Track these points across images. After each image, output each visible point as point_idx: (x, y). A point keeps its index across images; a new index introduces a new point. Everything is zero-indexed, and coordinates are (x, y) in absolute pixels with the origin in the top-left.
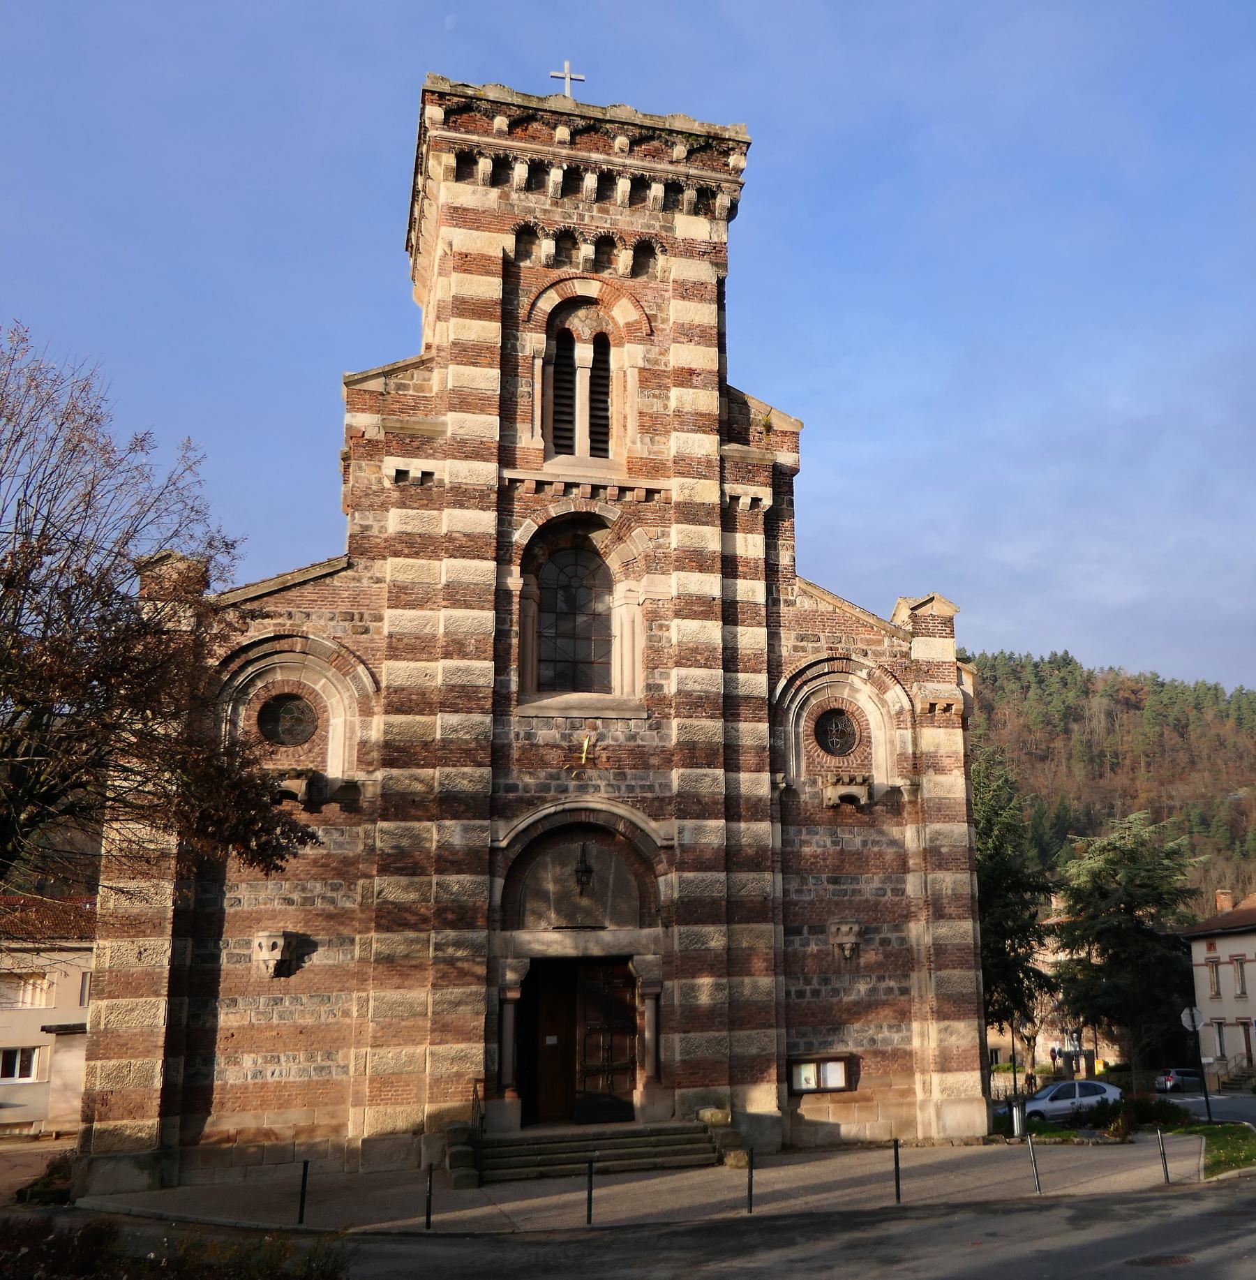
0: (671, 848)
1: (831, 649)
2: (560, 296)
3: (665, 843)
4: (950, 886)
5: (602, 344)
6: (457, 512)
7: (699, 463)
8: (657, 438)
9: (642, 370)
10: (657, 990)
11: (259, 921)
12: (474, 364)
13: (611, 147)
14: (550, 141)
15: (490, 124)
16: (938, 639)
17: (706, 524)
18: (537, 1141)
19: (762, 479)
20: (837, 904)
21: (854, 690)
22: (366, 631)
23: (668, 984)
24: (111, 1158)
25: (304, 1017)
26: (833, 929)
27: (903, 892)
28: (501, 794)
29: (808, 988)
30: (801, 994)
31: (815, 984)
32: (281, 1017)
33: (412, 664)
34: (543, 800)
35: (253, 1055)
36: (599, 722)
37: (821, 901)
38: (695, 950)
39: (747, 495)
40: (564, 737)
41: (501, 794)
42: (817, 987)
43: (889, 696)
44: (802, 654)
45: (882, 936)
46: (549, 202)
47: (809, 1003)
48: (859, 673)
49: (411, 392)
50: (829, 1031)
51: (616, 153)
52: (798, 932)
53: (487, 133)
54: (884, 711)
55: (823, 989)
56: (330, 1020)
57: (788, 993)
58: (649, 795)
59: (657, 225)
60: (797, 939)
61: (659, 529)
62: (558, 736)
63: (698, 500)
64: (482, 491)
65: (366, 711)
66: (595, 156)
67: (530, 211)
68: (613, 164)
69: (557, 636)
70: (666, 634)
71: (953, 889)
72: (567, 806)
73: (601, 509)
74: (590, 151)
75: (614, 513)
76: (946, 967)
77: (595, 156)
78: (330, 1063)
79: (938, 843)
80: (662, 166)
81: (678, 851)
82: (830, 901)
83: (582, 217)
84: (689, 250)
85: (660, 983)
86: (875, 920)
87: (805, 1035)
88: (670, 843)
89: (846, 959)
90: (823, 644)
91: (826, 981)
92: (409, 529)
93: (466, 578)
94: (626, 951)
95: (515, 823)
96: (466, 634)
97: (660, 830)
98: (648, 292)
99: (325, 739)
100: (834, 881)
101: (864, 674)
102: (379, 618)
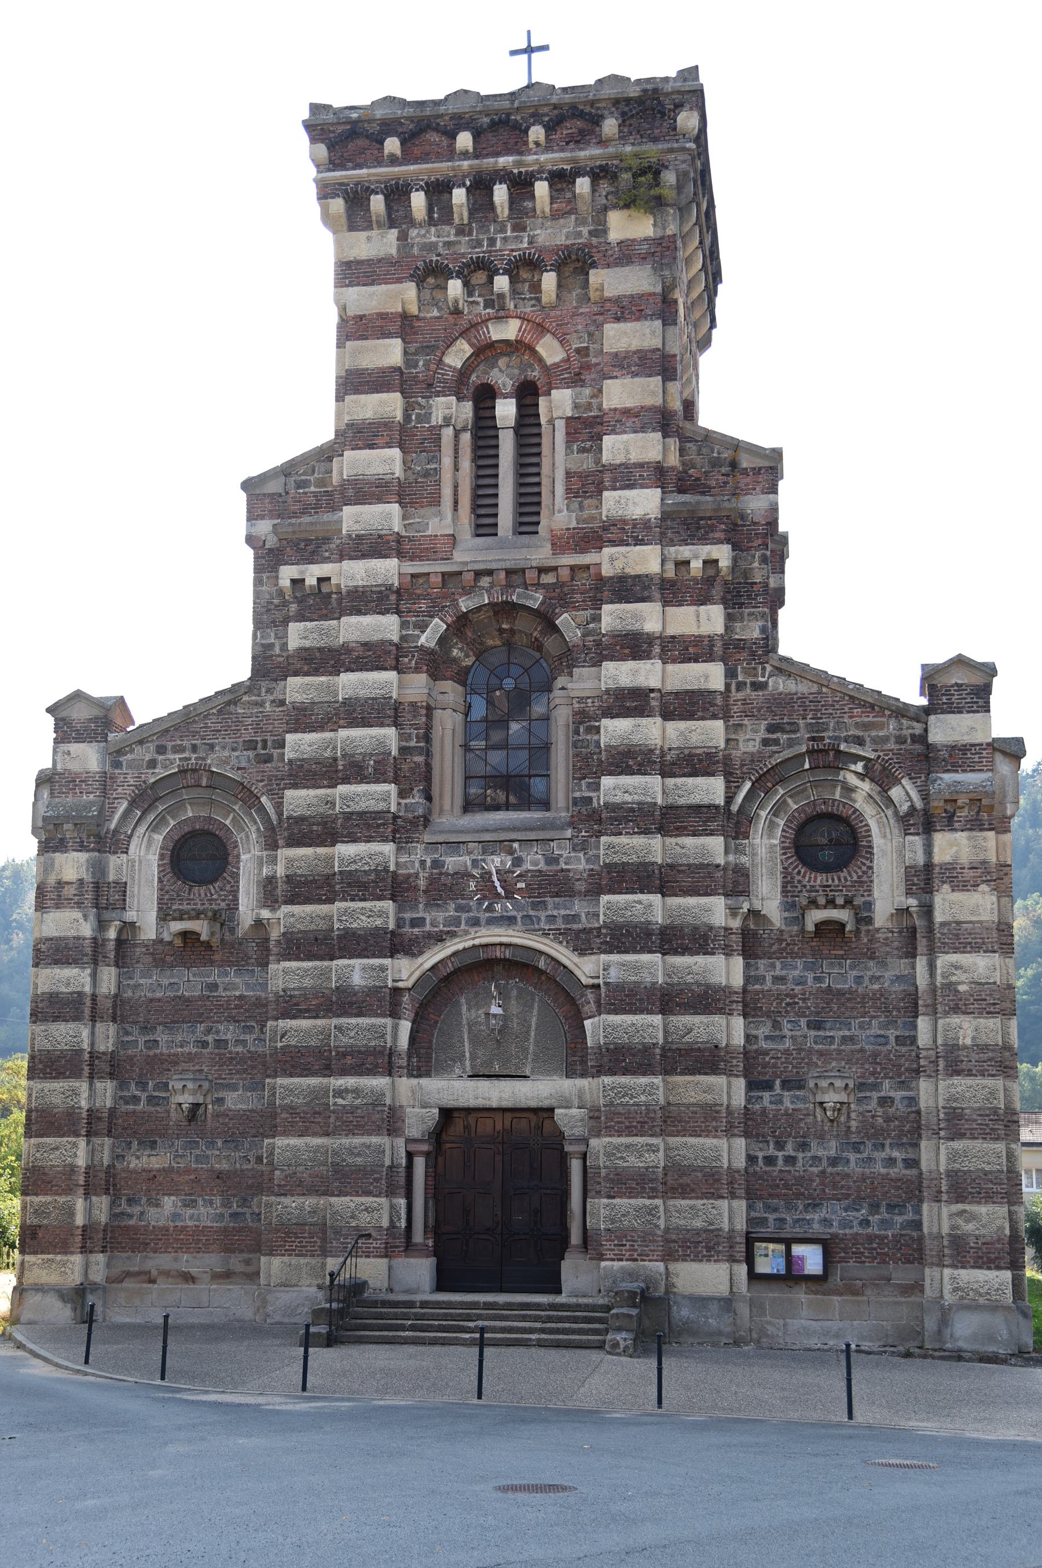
0: (598, 986)
1: (813, 739)
2: (471, 345)
3: (591, 981)
4: (970, 1033)
5: (528, 395)
6: (354, 620)
7: (634, 526)
8: (587, 502)
9: (569, 420)
10: (583, 1148)
11: (176, 1063)
12: (371, 447)
13: (526, 143)
14: (451, 153)
15: (381, 149)
16: (966, 715)
17: (643, 600)
18: (450, 1305)
19: (717, 535)
20: (821, 1054)
21: (849, 790)
22: (268, 759)
23: (594, 1142)
24: (37, 1290)
25: (219, 1162)
26: (811, 1084)
27: (913, 1040)
28: (407, 929)
29: (780, 1154)
30: (770, 1160)
31: (790, 1150)
32: (197, 1161)
33: (312, 792)
34: (453, 934)
35: (173, 1198)
36: (516, 845)
37: (799, 1050)
38: (621, 1104)
39: (696, 557)
40: (475, 863)
41: (407, 929)
42: (793, 1154)
43: (895, 793)
44: (775, 748)
45: (883, 1094)
46: (453, 231)
47: (781, 1171)
48: (853, 767)
49: (312, 489)
50: (806, 1207)
51: (540, 150)
52: (768, 1086)
53: (379, 162)
54: (890, 812)
55: (800, 1155)
56: (245, 1167)
57: (751, 1159)
58: (575, 926)
59: (585, 230)
60: (766, 1095)
61: (589, 613)
62: (469, 863)
63: (630, 571)
64: (380, 592)
65: (272, 845)
66: (505, 161)
67: (431, 247)
68: (528, 165)
69: (488, 748)
70: (596, 737)
71: (974, 1038)
72: (477, 942)
73: (519, 596)
74: (498, 154)
75: (536, 600)
76: (962, 1136)
77: (505, 161)
78: (245, 1210)
79: (954, 979)
80: (590, 153)
81: (603, 990)
82: (810, 1051)
83: (492, 241)
84: (626, 254)
85: (585, 1141)
86: (873, 1074)
87: (775, 1210)
88: (596, 981)
89: (832, 1121)
90: (804, 734)
91: (803, 1146)
92: (307, 644)
93: (363, 693)
94: (546, 1104)
95: (420, 960)
96: (364, 755)
97: (586, 968)
98: (579, 319)
99: (236, 876)
100: (817, 1025)
101: (859, 767)
102: (281, 744)
